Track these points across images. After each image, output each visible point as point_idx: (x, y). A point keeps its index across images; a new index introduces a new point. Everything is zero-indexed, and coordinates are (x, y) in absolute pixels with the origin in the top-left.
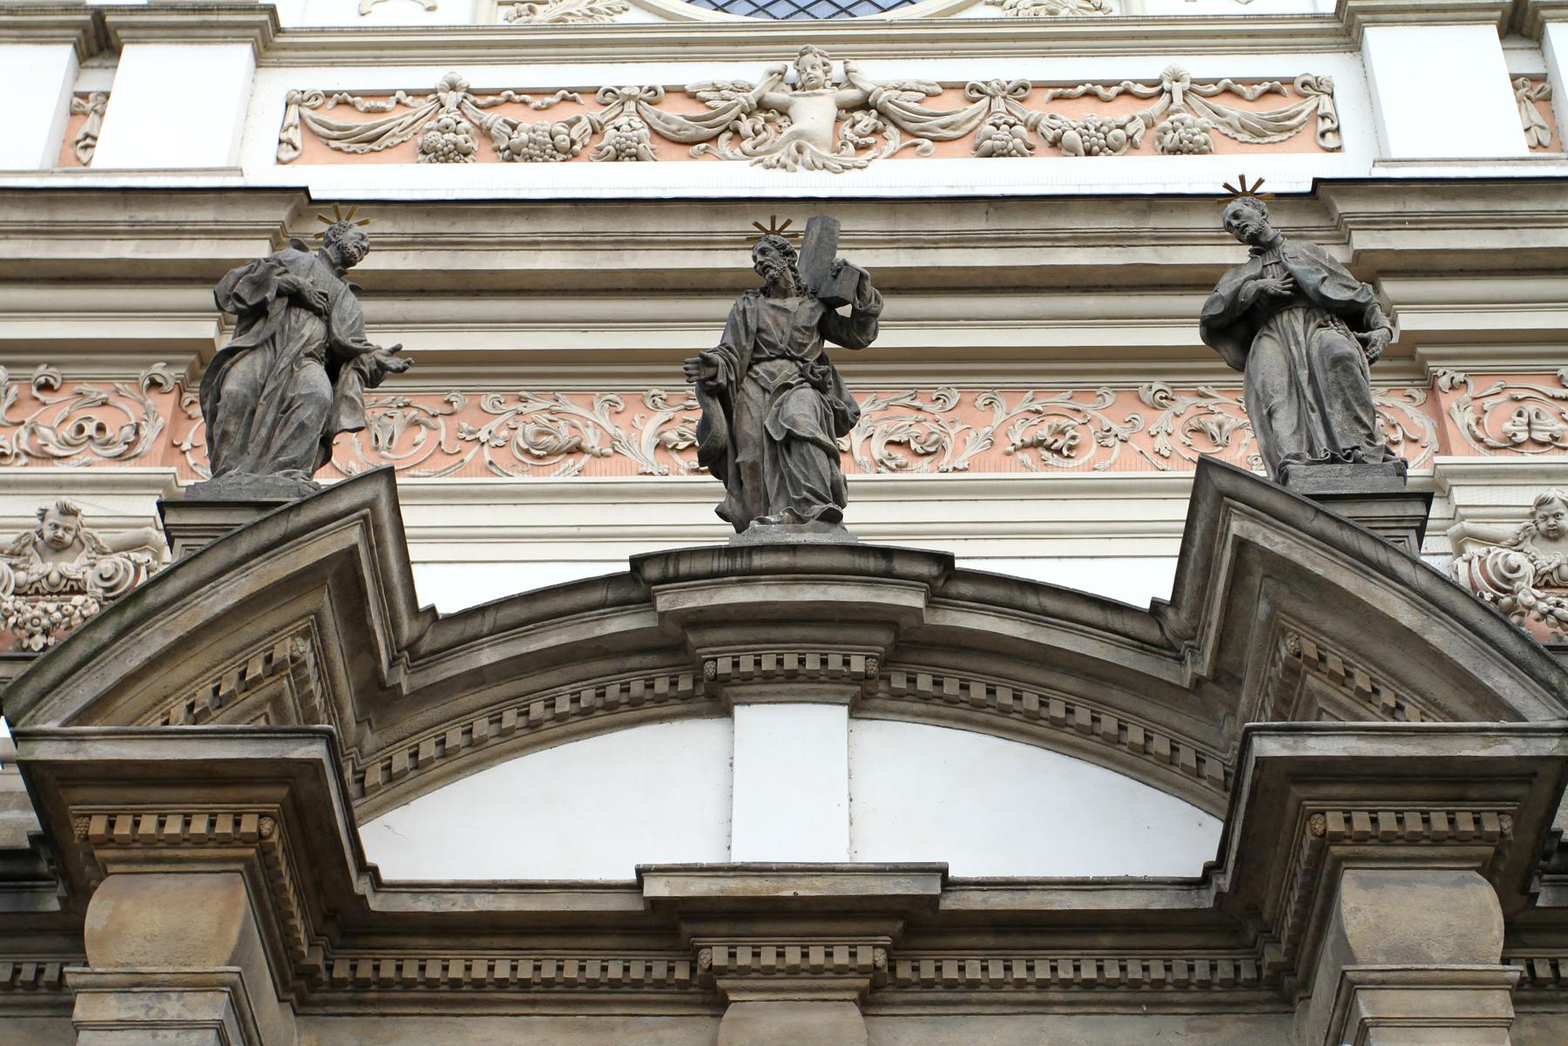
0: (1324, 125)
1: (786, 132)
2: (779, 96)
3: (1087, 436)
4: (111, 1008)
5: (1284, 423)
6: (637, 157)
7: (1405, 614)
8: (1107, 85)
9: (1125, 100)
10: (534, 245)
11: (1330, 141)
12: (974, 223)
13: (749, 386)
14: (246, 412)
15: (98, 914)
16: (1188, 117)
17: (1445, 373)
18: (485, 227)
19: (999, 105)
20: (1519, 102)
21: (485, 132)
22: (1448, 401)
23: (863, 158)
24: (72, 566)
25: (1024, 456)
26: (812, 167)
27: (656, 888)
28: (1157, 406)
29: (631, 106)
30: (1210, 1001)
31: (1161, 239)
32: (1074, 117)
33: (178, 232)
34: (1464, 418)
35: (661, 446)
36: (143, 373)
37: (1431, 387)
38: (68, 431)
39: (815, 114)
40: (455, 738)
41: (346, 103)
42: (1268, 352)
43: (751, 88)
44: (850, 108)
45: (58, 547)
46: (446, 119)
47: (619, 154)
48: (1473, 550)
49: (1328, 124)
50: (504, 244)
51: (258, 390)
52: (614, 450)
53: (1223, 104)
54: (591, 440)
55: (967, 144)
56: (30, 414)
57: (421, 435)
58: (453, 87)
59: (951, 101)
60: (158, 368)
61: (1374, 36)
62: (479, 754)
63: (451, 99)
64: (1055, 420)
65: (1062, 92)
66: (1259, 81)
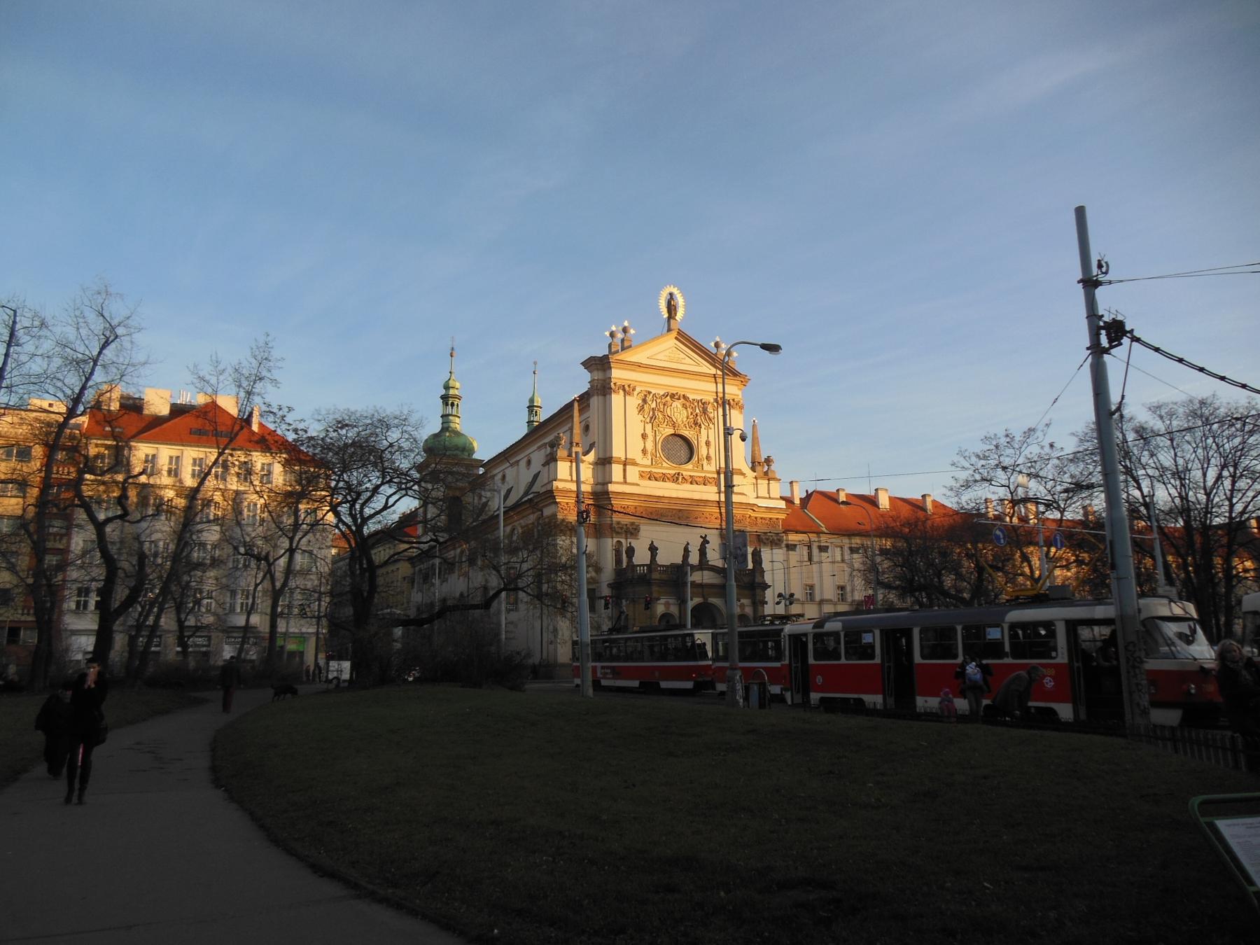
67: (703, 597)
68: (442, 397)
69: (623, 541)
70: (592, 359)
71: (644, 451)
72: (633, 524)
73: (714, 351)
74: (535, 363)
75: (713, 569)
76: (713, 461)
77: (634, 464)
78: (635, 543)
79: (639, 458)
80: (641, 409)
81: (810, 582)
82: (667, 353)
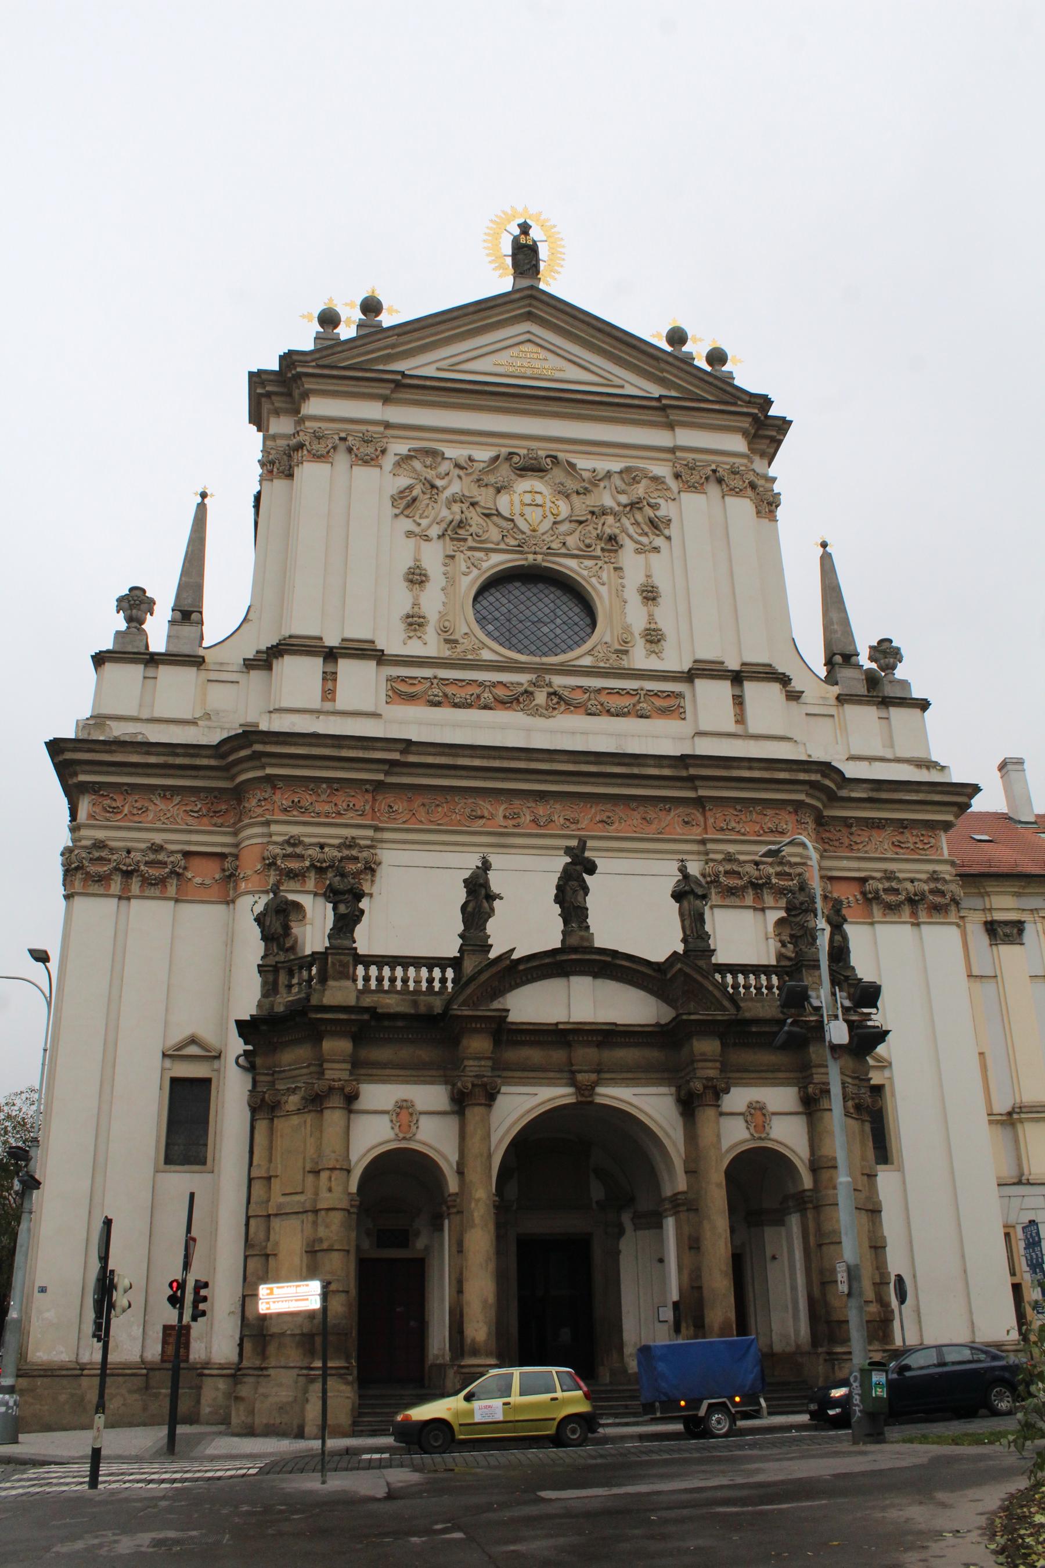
0: (682, 710)
1: (534, 703)
2: (530, 689)
3: (615, 818)
4: (471, 1063)
5: (687, 923)
6: (491, 709)
7: (711, 988)
8: (623, 689)
9: (627, 696)
10: (472, 757)
11: (683, 716)
12: (592, 759)
13: (568, 888)
15: (465, 1042)
16: (644, 705)
18: (460, 751)
19: (592, 695)
20: (734, 704)
21: (446, 695)
22: (708, 814)
23: (556, 712)
24: (354, 852)
25: (600, 825)
26: (540, 716)
27: (561, 1027)
28: (634, 810)
29: (487, 690)
31: (639, 765)
32: (615, 702)
33: (374, 749)
34: (711, 821)
35: (505, 817)
36: (364, 787)
37: (704, 808)
38: (345, 805)
39: (541, 698)
40: (513, 983)
41: (403, 680)
42: (685, 903)
43: (522, 684)
44: (550, 694)
45: (350, 847)
46: (436, 691)
47: (486, 707)
48: (711, 864)
49: (682, 710)
50: (464, 756)
51: (474, 909)
52: (492, 817)
53: (654, 700)
54: (486, 814)
55: (582, 710)
56: (334, 799)
57: (440, 809)
58: (435, 677)
59: (579, 691)
60: (368, 786)
61: (698, 682)
62: (518, 985)
63: (435, 681)
64: (608, 814)
65: (612, 692)
66: (664, 692)
67: (573, 1083)
71: (414, 623)
72: (350, 844)
76: (669, 646)
79: (393, 641)
80: (406, 503)
82: (503, 358)
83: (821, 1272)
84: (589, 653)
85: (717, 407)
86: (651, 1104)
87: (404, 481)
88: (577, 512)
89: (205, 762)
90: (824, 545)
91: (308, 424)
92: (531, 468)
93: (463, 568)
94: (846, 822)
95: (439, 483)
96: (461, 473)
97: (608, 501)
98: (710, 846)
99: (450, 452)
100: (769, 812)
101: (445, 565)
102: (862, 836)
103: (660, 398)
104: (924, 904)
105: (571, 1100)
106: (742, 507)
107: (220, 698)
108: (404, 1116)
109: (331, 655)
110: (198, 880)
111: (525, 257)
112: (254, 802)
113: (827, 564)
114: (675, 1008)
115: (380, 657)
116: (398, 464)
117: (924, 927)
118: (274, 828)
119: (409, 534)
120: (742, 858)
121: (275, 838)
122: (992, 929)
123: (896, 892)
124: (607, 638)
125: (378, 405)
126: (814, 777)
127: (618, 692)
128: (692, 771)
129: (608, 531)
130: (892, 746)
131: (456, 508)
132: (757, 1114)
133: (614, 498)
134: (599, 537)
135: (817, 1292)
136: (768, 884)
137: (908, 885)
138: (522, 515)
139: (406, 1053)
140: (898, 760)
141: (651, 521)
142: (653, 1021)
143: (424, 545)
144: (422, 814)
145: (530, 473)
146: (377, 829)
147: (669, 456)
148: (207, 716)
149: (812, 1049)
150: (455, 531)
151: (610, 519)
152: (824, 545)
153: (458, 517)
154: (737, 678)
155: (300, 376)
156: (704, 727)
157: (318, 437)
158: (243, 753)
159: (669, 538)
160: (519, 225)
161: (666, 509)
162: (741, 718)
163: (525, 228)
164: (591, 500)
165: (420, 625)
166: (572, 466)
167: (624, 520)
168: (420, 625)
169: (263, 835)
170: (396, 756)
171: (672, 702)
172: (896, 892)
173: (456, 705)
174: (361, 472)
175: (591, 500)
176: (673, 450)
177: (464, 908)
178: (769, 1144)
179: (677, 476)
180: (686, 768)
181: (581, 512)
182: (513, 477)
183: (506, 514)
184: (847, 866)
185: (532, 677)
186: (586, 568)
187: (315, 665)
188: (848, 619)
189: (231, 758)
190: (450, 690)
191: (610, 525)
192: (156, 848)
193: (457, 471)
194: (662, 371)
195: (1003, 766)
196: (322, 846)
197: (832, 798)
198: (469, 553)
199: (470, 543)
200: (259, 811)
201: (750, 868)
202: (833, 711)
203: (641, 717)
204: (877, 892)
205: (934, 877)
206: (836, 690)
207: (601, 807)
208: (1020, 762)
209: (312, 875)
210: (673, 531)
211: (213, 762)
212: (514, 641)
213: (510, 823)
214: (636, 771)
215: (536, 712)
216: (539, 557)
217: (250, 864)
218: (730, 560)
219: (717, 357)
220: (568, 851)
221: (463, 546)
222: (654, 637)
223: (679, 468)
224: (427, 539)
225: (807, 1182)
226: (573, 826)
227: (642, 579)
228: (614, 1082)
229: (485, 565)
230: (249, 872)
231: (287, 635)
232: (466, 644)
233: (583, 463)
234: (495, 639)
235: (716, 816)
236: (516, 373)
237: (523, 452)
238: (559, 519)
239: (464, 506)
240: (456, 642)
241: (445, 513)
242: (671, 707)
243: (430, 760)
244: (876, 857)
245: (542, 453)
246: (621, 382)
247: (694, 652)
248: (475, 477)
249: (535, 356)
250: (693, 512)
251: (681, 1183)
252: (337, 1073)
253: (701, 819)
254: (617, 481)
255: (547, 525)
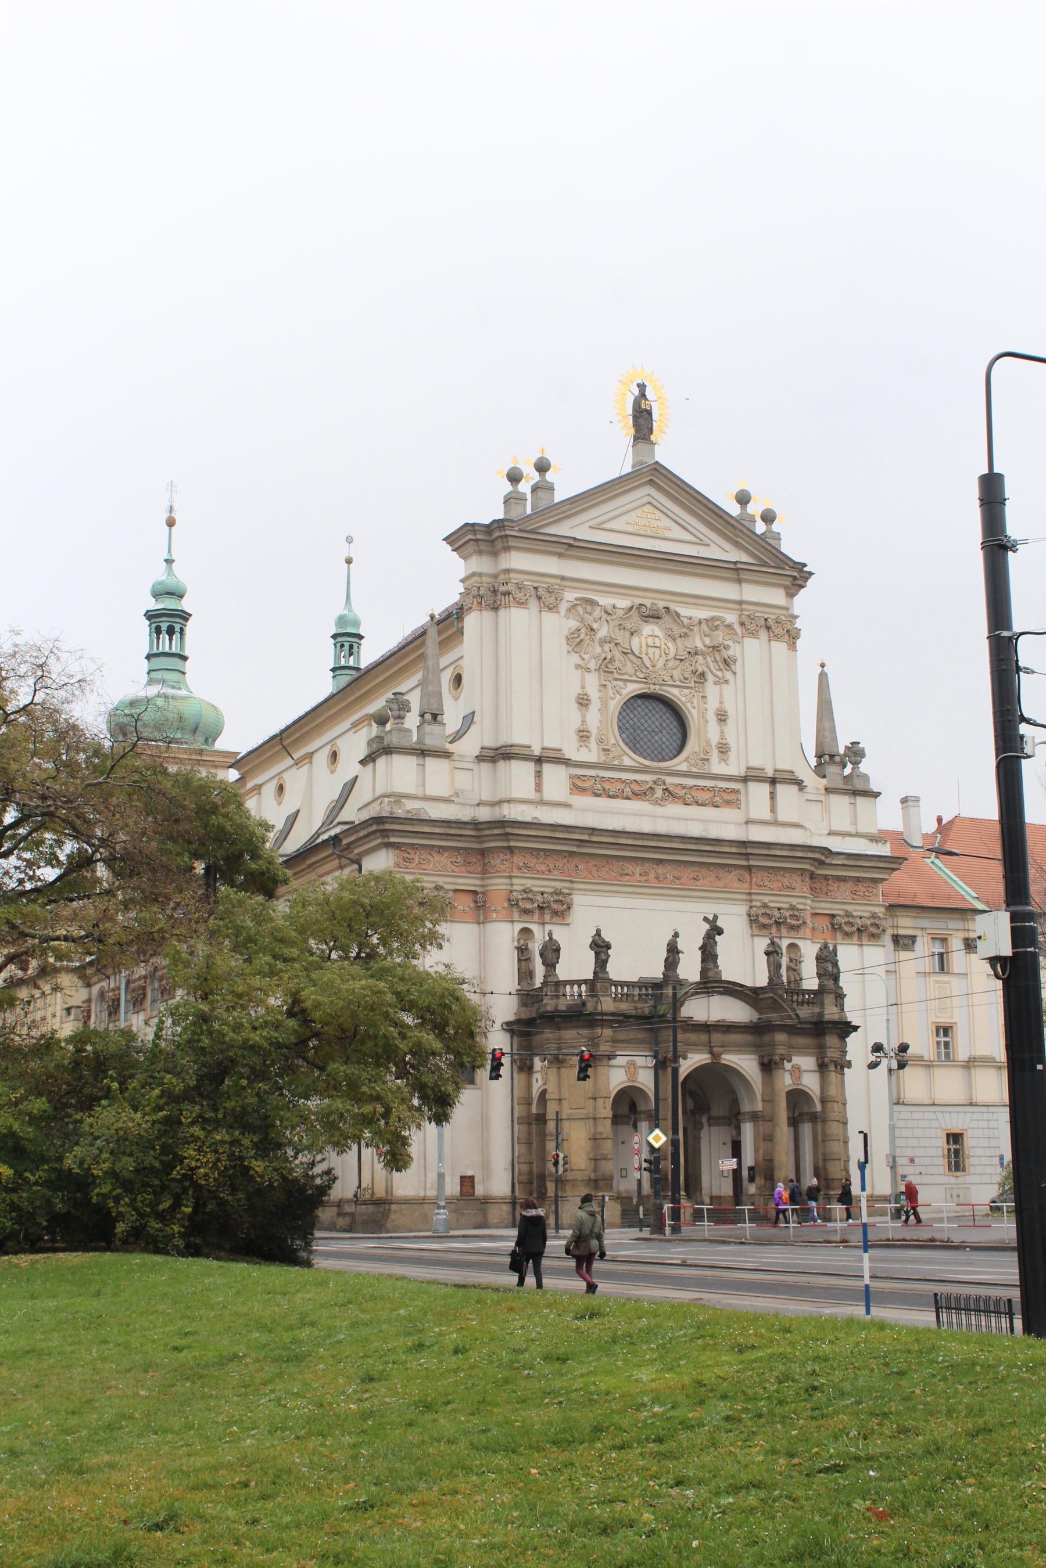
14: (671, 963)
17: (754, 870)
30: (752, 1034)
34: (754, 880)
37: (750, 871)
39: (659, 793)
42: (772, 958)
46: (599, 787)
47: (628, 798)
56: (547, 862)
67: (711, 1053)
68: (150, 616)
69: (534, 927)
70: (470, 528)
71: (583, 735)
72: (557, 892)
73: (733, 509)
74: (350, 540)
75: (734, 990)
76: (732, 755)
77: (561, 760)
78: (560, 935)
79: (572, 752)
80: (575, 642)
81: (944, 1020)
82: (632, 517)
83: (824, 1154)
84: (686, 760)
85: (771, 570)
86: (746, 1063)
87: (573, 624)
88: (681, 652)
89: (468, 833)
90: (823, 666)
91: (512, 575)
92: (653, 616)
93: (611, 694)
94: (826, 878)
95: (595, 626)
96: (609, 618)
97: (699, 644)
98: (754, 897)
99: (604, 600)
100: (787, 875)
101: (600, 691)
102: (834, 886)
103: (735, 563)
104: (866, 932)
105: (709, 1061)
106: (780, 648)
107: (463, 780)
108: (632, 1069)
109: (539, 760)
110: (461, 908)
111: (642, 421)
112: (499, 861)
113: (823, 677)
114: (761, 1014)
115: (566, 762)
116: (569, 610)
117: (865, 948)
118: (515, 881)
119: (578, 667)
120: (771, 905)
121: (515, 888)
122: (896, 939)
123: (851, 924)
124: (697, 750)
125: (555, 559)
126: (817, 856)
127: (703, 789)
128: (749, 851)
129: (700, 670)
130: (856, 824)
131: (607, 647)
132: (797, 1070)
133: (702, 640)
134: (694, 672)
135: (820, 1164)
136: (785, 922)
137: (859, 921)
138: (647, 654)
139: (632, 1035)
140: (858, 835)
141: (725, 661)
142: (748, 1021)
143: (587, 675)
144: (595, 873)
145: (651, 620)
146: (571, 882)
147: (737, 607)
148: (457, 794)
149: (827, 1038)
150: (606, 667)
151: (700, 657)
152: (823, 666)
153: (609, 657)
154: (773, 781)
155: (506, 536)
156: (753, 816)
157: (520, 587)
158: (496, 831)
159: (735, 673)
160: (638, 385)
161: (734, 651)
162: (773, 810)
163: (642, 387)
164: (689, 644)
165: (587, 737)
166: (678, 615)
167: (709, 659)
168: (587, 737)
169: (506, 884)
170: (585, 837)
171: (734, 797)
172: (851, 924)
173: (610, 797)
174: (547, 616)
175: (689, 644)
176: (740, 603)
177: (666, 960)
178: (801, 1087)
179: (742, 624)
180: (746, 848)
181: (683, 654)
182: (640, 622)
183: (637, 653)
184: (825, 907)
185: (654, 777)
186: (685, 695)
187: (530, 767)
188: (834, 727)
189: (486, 832)
190: (607, 787)
191: (700, 665)
192: (438, 888)
193: (605, 616)
194: (737, 536)
195: (904, 801)
196: (542, 894)
197: (821, 863)
198: (615, 683)
199: (616, 676)
200: (503, 867)
201: (776, 913)
202: (822, 798)
203: (716, 807)
204: (841, 924)
205: (874, 916)
206: (824, 781)
207: (694, 869)
208: (917, 800)
209: (537, 912)
210: (738, 668)
211: (472, 833)
212: (638, 746)
213: (643, 878)
214: (717, 849)
215: (656, 803)
216: (657, 687)
217: (498, 903)
218: (772, 691)
219: (768, 517)
220: (705, 919)
221: (610, 677)
222: (723, 749)
223: (744, 619)
224: (588, 670)
225: (818, 1107)
226: (678, 882)
227: (717, 705)
228: (729, 1052)
229: (624, 692)
230: (499, 908)
231: (509, 742)
232: (615, 752)
233: (684, 611)
234: (627, 744)
235: (757, 877)
236: (641, 532)
237: (648, 603)
238: (669, 657)
239: (612, 645)
240: (608, 750)
241: (598, 650)
242: (729, 799)
243: (604, 839)
244: (843, 902)
245: (661, 604)
246: (709, 542)
247: (747, 761)
248: (617, 623)
249: (653, 516)
250: (751, 651)
251: (759, 1106)
252: (604, 1048)
253: (748, 877)
254: (704, 626)
255: (660, 664)
